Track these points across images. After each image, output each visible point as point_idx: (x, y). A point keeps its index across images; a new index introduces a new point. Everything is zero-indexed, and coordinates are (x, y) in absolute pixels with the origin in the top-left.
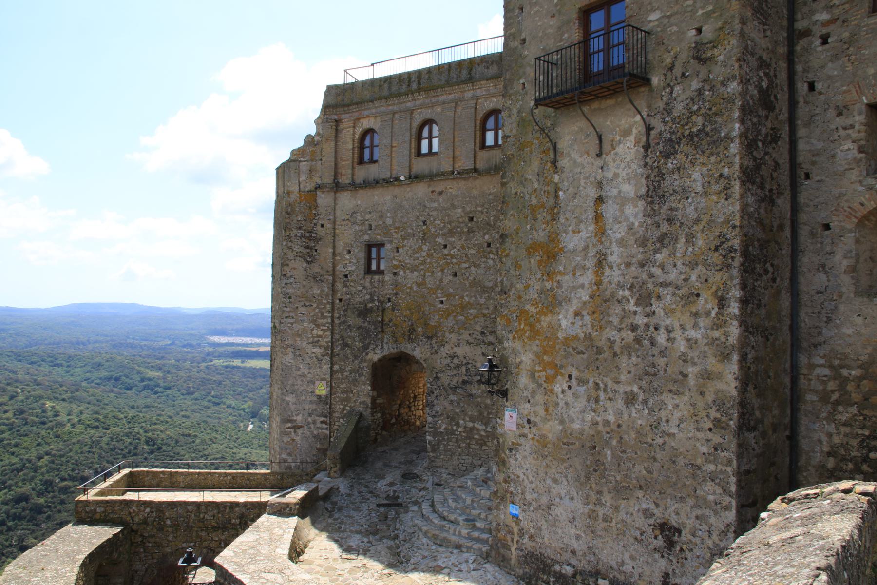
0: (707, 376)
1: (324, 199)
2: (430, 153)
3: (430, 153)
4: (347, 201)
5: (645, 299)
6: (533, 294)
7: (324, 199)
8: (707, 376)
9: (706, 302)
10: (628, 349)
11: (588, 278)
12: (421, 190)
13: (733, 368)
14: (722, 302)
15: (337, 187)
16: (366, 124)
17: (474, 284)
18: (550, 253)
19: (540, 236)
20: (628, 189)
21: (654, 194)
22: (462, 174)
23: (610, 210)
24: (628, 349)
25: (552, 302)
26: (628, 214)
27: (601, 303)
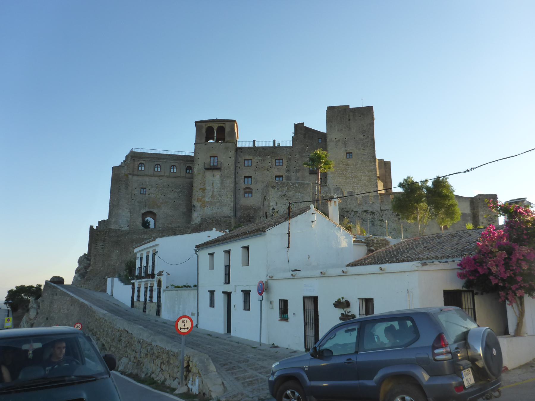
0: (229, 204)
1: (130, 176)
2: (158, 171)
3: (158, 171)
4: (135, 178)
5: (220, 196)
6: (200, 195)
7: (130, 176)
8: (229, 204)
9: (229, 196)
10: (217, 202)
11: (211, 193)
12: (156, 178)
13: (232, 203)
14: (231, 196)
15: (133, 175)
16: (141, 162)
17: (169, 198)
18: (204, 190)
19: (202, 187)
20: (218, 182)
21: (222, 182)
22: (167, 177)
23: (214, 184)
24: (217, 202)
25: (204, 197)
26: (217, 185)
27: (213, 196)
